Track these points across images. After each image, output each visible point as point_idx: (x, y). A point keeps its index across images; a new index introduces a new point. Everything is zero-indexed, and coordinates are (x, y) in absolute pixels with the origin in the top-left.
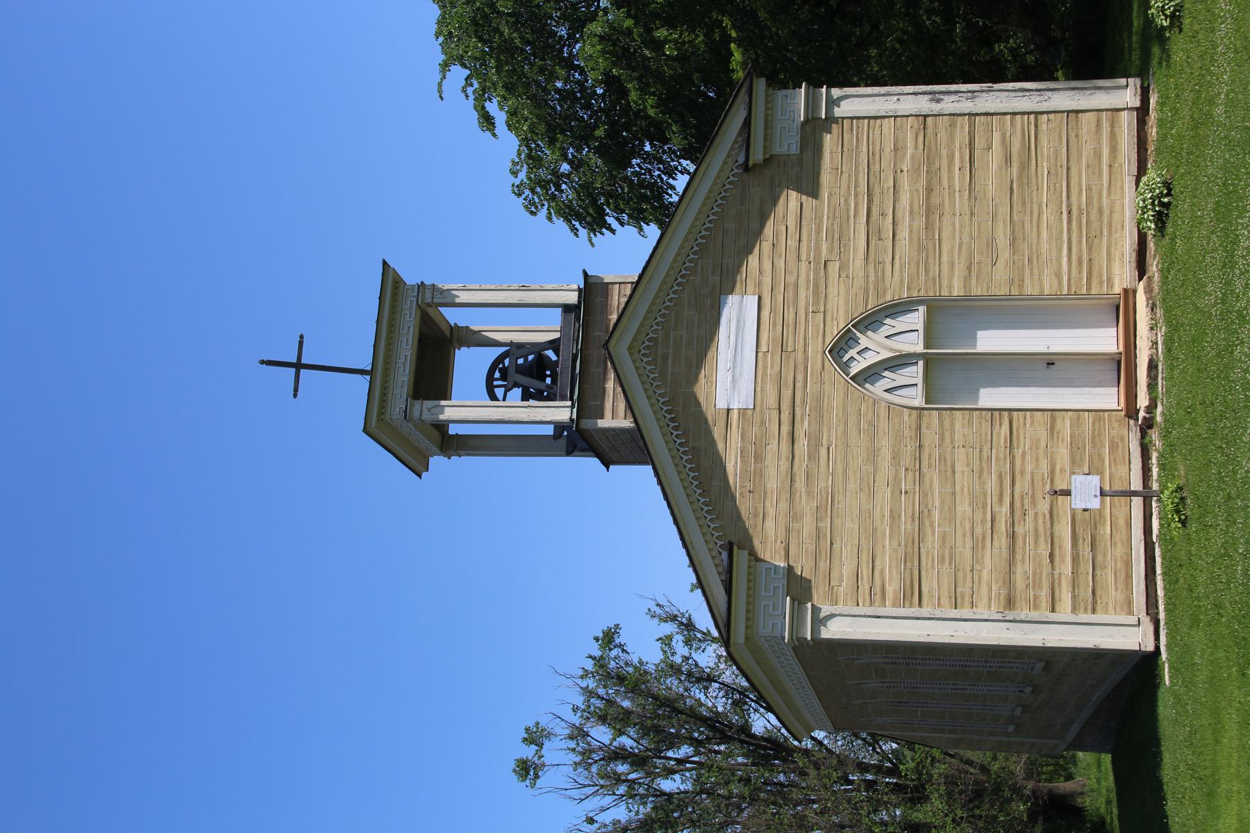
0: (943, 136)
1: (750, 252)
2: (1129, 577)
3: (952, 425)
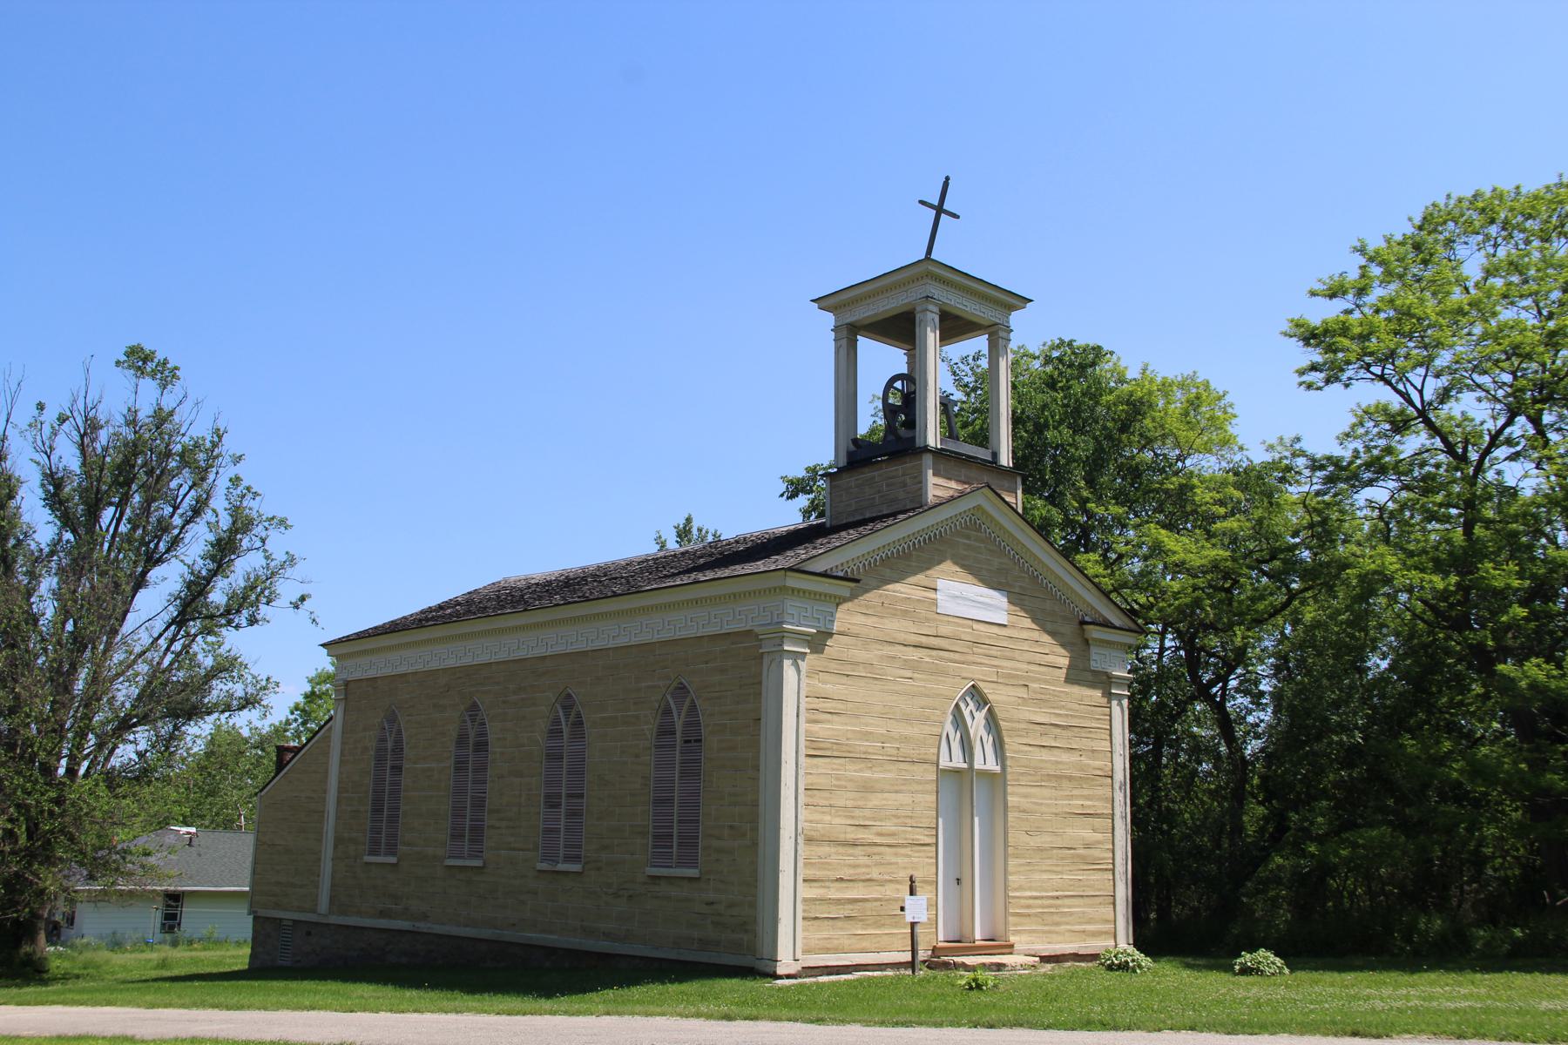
0: (1100, 791)
1: (1034, 620)
2: (827, 950)
3: (923, 792)
